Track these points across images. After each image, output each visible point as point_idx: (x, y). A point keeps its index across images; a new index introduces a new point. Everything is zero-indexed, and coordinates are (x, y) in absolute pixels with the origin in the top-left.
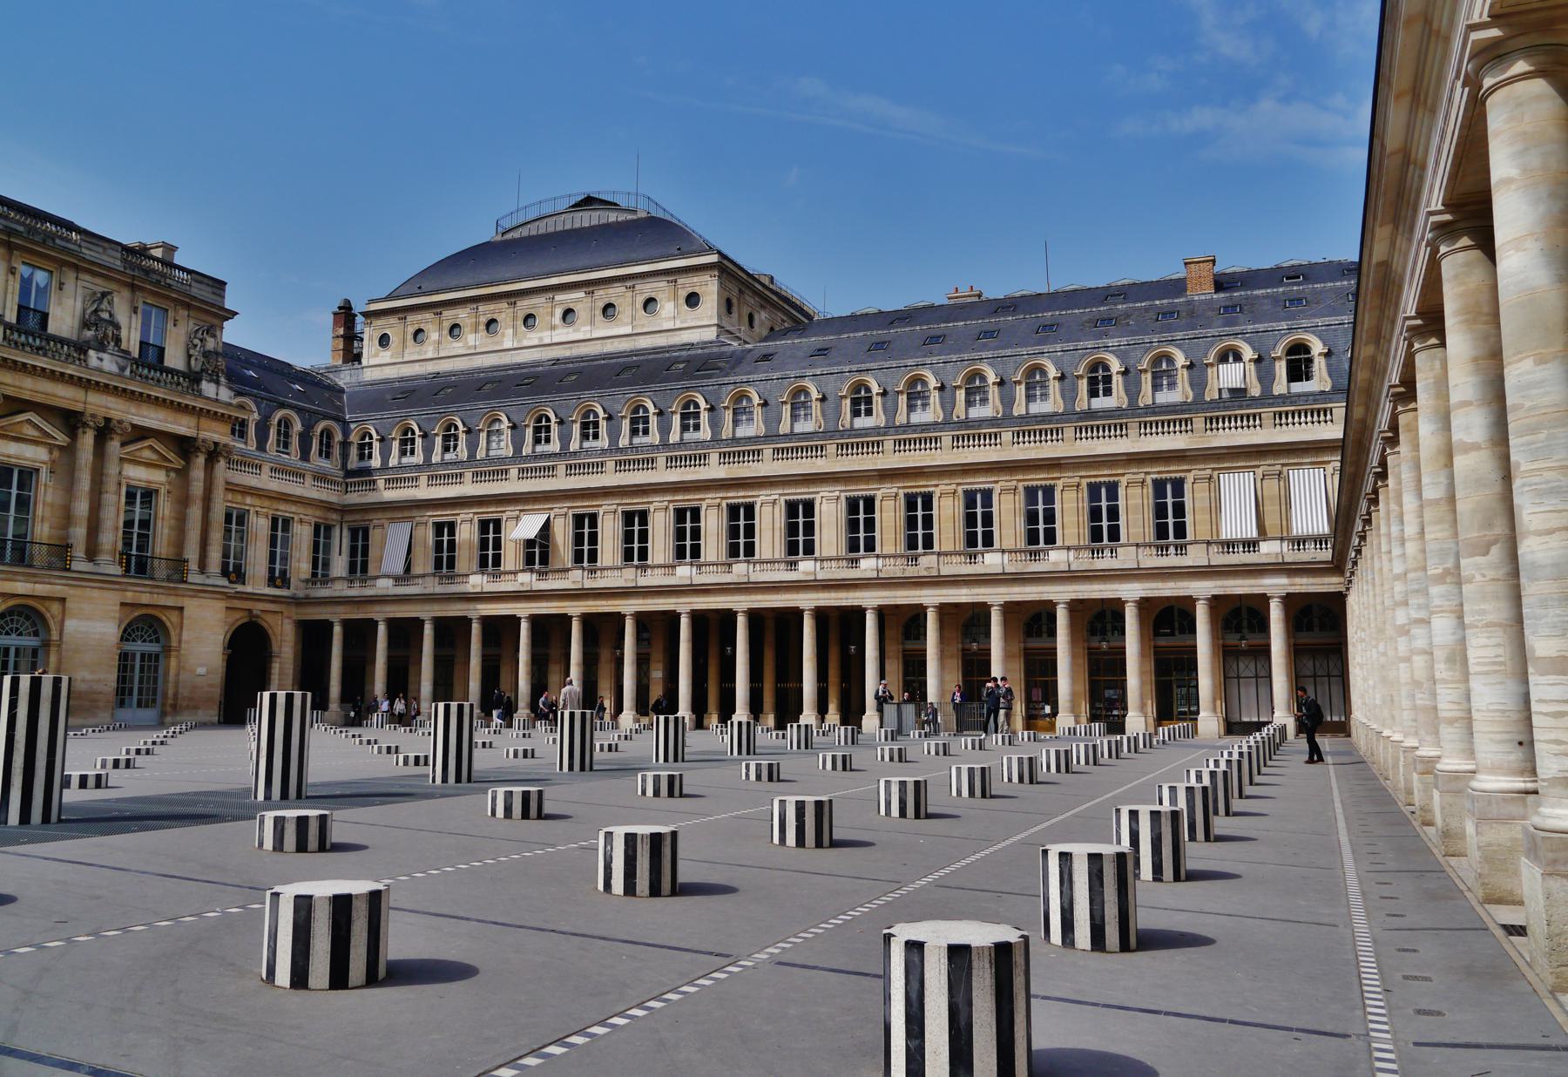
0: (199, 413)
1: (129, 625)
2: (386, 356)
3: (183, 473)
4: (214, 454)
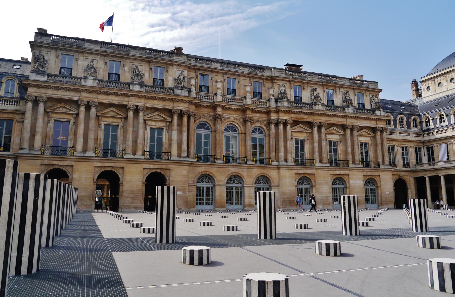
0: (376, 120)
1: (366, 181)
2: (430, 93)
3: (374, 137)
4: (382, 130)
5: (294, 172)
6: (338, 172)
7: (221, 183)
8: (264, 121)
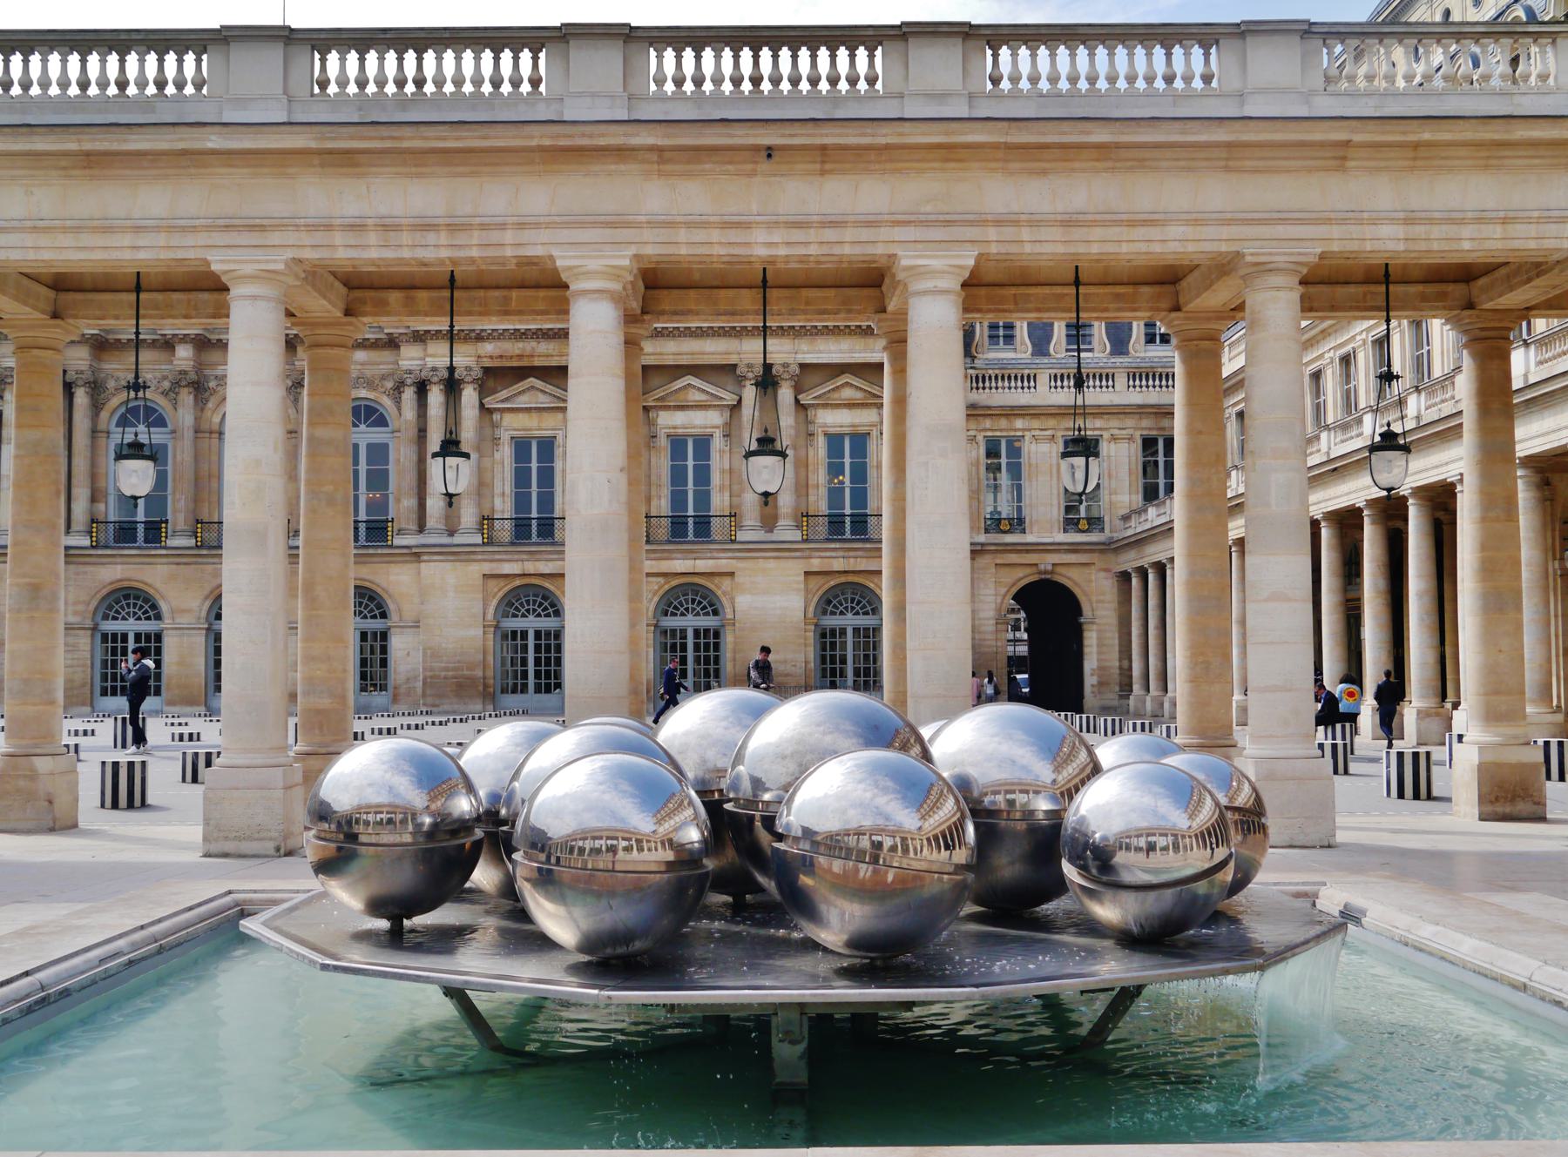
5: (476, 570)
6: (680, 565)
7: (184, 620)
8: (383, 378)
